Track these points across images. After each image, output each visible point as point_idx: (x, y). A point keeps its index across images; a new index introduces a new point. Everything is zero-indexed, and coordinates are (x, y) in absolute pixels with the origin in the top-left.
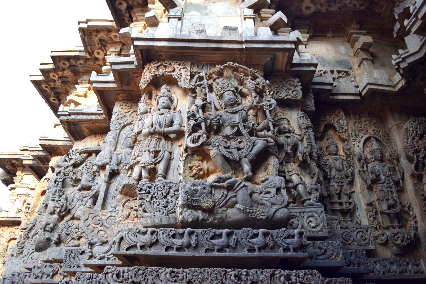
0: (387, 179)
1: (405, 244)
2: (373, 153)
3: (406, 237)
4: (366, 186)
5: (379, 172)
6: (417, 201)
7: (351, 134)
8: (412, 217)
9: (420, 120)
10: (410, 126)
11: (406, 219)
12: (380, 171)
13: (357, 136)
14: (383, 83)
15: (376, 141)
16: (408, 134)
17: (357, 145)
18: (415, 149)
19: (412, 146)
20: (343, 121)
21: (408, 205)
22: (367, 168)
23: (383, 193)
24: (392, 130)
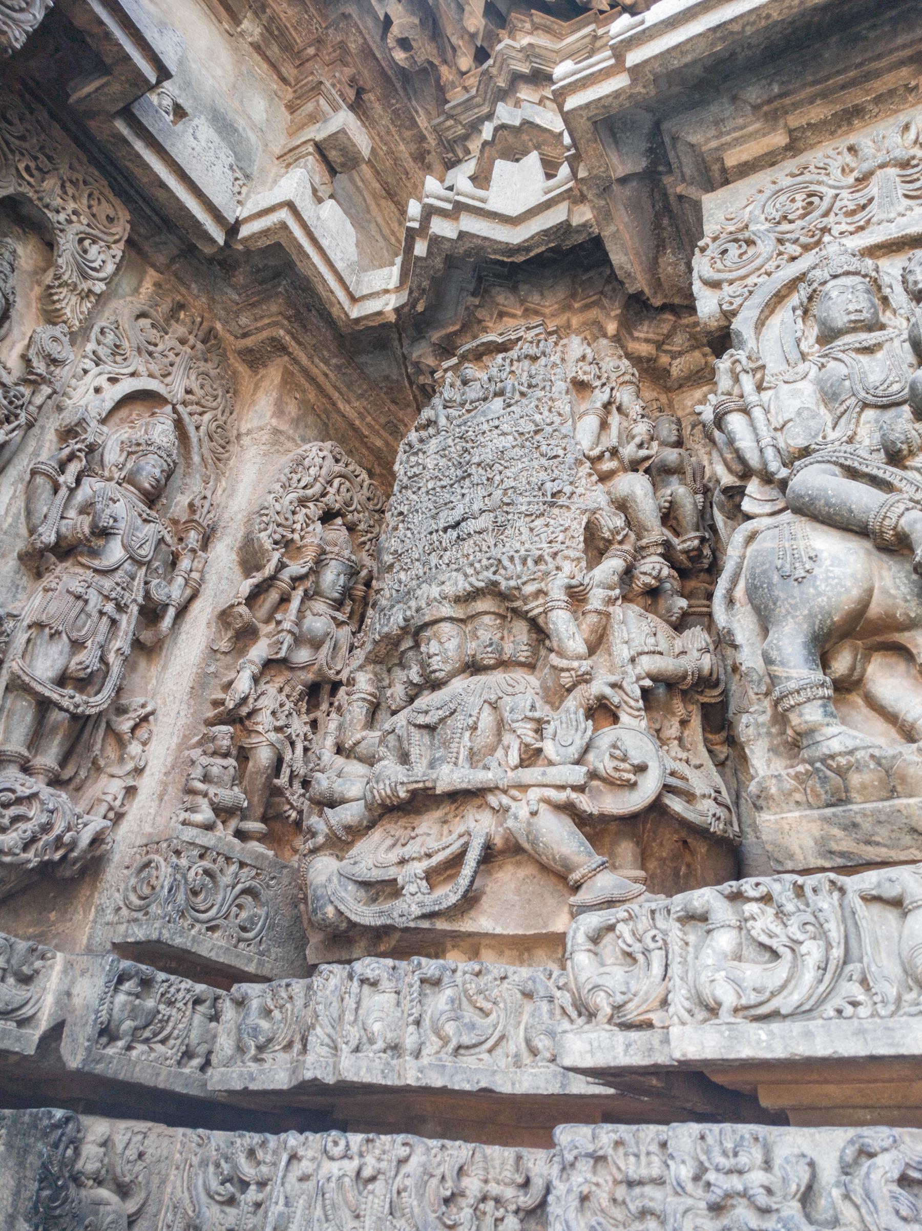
0: (127, 566)
1: (29, 861)
2: (136, 452)
3: (57, 831)
4: (20, 545)
5: (115, 520)
6: (182, 713)
7: (102, 332)
8: (130, 766)
9: (351, 468)
10: (316, 459)
11: (102, 763)
12: (122, 525)
13: (118, 358)
14: (332, 257)
15: (175, 420)
16: (296, 477)
17: (96, 383)
18: (290, 536)
19: (287, 519)
20: (102, 257)
21: (142, 712)
22: (78, 481)
23: (78, 610)
24: (246, 440)
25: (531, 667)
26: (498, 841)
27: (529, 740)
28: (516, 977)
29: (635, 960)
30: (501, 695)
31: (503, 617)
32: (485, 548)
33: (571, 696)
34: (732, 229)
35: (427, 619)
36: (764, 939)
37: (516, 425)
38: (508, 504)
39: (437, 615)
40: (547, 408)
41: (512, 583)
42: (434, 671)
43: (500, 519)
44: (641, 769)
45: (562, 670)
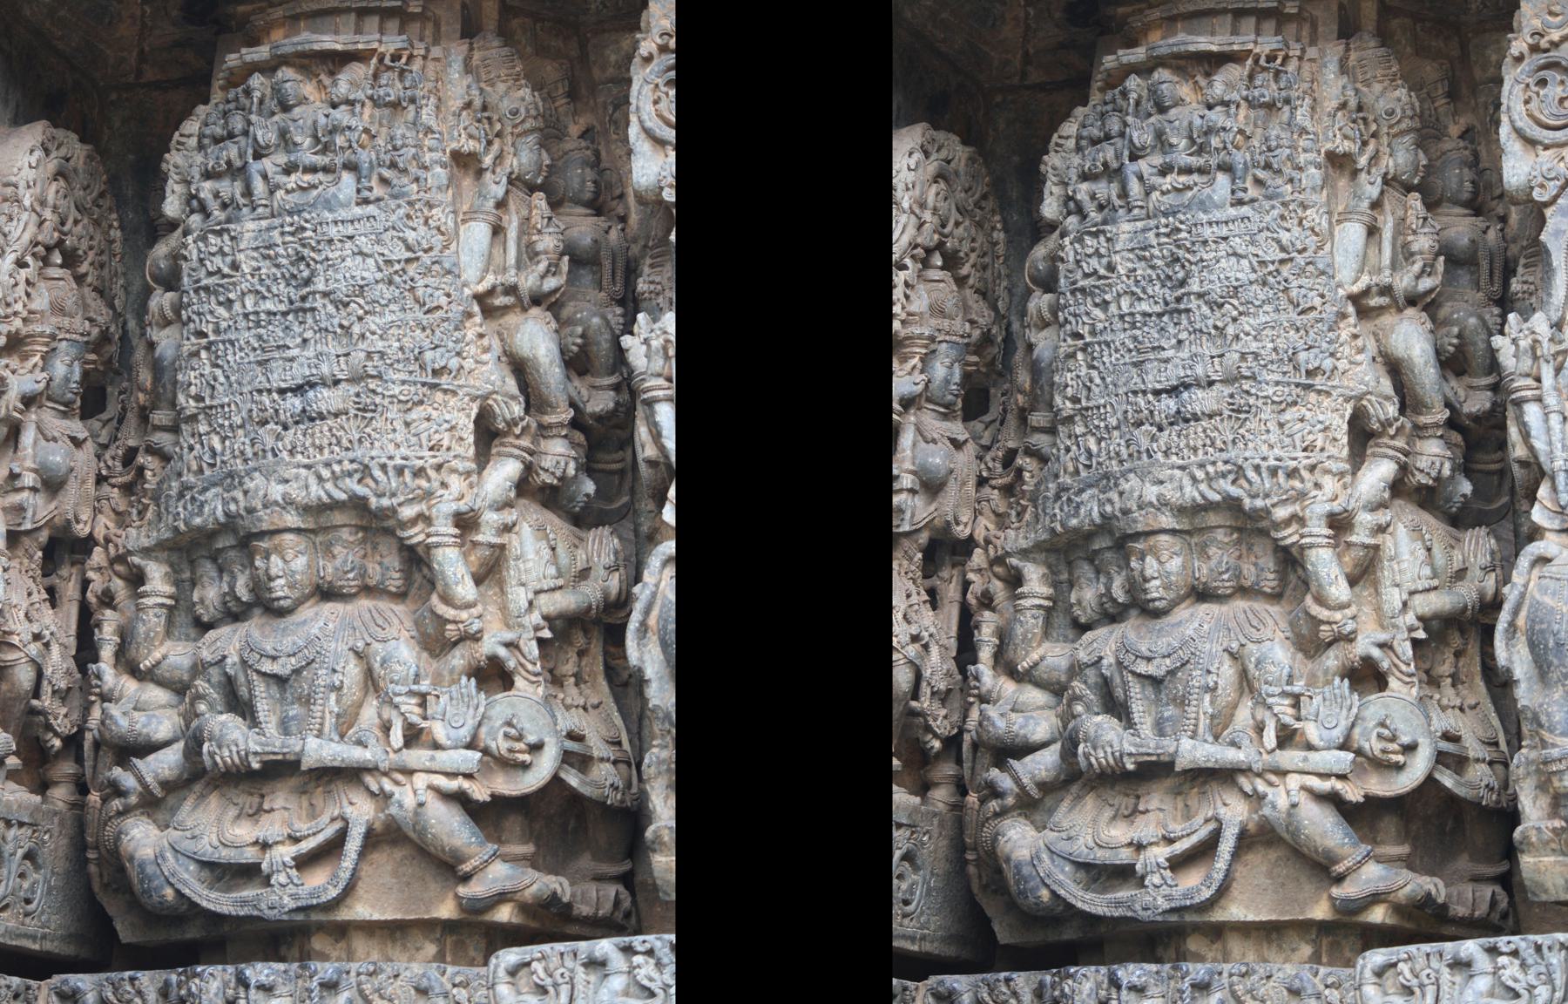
25: (1276, 597)
26: (1251, 827)
27: (1288, 720)
28: (1281, 975)
29: (1412, 993)
30: (1244, 641)
31: (1239, 530)
32: (1219, 443)
33: (1331, 653)
34: (1555, 36)
35: (1140, 527)
36: (1510, 983)
37: (1253, 243)
38: (1246, 378)
39: (1156, 527)
40: (1296, 222)
41: (1259, 503)
42: (1154, 600)
43: (1239, 400)
44: (1410, 749)
45: (1322, 622)
